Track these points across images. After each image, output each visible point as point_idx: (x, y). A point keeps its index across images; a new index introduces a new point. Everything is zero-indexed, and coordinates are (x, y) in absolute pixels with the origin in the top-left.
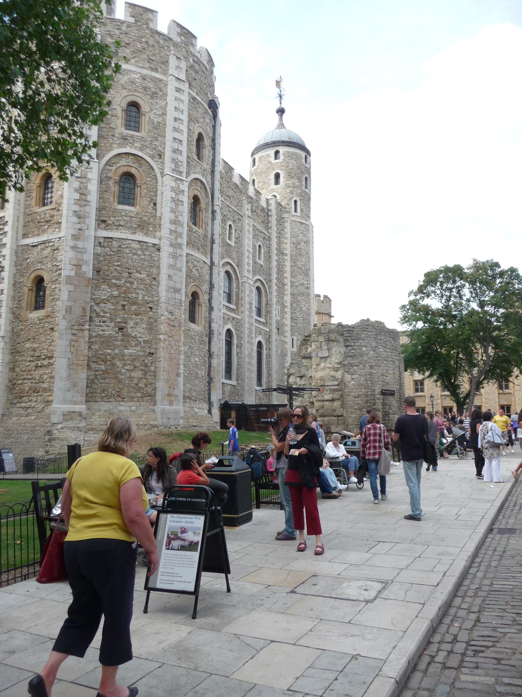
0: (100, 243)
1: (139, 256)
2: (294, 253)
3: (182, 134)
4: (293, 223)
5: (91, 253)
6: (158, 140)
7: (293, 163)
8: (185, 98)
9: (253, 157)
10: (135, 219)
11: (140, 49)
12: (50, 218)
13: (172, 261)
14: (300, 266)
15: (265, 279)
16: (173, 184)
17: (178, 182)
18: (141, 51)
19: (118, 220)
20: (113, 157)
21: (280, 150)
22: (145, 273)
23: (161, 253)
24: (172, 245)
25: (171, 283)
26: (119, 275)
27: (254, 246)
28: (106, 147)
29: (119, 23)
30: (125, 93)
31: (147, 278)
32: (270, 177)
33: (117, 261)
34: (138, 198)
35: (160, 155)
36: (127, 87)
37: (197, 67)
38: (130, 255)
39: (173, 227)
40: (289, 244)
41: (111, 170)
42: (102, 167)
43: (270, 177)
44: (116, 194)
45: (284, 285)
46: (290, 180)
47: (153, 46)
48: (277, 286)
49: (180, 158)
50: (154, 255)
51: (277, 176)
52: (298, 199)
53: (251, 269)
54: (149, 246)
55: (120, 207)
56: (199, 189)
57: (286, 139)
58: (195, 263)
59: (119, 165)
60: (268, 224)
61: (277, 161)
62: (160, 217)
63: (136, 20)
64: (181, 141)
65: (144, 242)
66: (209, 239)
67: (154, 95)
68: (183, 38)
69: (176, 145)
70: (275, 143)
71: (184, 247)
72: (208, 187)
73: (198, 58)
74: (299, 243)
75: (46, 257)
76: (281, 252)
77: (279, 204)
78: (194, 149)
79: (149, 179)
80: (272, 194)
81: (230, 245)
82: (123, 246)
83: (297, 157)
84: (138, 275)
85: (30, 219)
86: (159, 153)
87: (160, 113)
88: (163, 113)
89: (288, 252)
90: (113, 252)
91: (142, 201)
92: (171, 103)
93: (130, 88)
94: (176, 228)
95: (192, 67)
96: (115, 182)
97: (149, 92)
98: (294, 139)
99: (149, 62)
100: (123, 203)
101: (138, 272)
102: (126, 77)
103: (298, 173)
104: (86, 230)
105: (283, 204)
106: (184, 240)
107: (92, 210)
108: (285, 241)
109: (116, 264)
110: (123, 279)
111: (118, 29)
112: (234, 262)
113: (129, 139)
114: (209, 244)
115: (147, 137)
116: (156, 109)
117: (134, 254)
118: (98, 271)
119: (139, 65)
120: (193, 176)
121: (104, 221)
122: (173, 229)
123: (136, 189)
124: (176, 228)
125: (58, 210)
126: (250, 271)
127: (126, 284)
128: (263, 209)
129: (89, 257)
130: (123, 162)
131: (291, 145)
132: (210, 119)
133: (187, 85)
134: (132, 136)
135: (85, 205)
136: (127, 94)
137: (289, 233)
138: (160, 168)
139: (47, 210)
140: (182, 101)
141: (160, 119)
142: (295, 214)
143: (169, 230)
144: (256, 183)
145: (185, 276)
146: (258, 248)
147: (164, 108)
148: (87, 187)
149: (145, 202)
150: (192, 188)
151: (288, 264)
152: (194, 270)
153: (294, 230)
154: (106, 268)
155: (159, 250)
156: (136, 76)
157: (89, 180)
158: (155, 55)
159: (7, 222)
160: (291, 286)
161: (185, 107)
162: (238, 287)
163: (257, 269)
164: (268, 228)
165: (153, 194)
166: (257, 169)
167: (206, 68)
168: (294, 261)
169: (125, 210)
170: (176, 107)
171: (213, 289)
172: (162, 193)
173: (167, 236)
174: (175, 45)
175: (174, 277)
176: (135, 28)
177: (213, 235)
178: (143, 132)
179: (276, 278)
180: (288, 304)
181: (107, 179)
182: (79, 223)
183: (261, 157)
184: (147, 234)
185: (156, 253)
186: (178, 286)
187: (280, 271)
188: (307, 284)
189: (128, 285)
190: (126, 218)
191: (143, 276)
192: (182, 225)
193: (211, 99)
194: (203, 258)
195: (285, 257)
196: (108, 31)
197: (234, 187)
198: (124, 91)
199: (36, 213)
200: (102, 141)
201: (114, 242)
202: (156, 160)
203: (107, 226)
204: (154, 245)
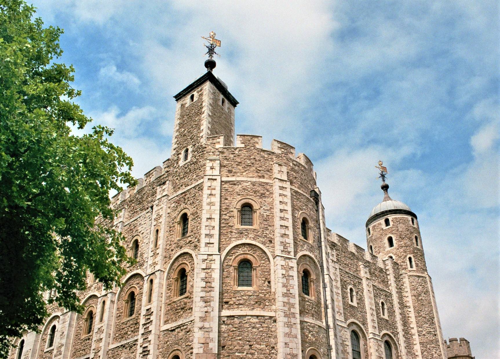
0: (224, 321)
1: (258, 329)
2: (416, 304)
3: (288, 221)
4: (411, 278)
5: (216, 332)
6: (268, 229)
7: (401, 227)
8: (288, 193)
9: (368, 227)
10: (252, 297)
11: (250, 164)
12: (184, 305)
13: (287, 330)
14: (424, 315)
15: (392, 333)
16: (283, 263)
17: (287, 261)
18: (251, 166)
19: (238, 300)
20: (232, 248)
21: (389, 218)
22: (264, 344)
23: (277, 324)
24: (286, 316)
25: (288, 351)
26: (241, 348)
27: (377, 304)
29: (233, 150)
30: (239, 198)
31: (267, 348)
32: (385, 242)
33: (239, 336)
34: (255, 279)
35: (271, 241)
36: (241, 193)
37: (297, 168)
38: (250, 329)
39: (286, 300)
40: (410, 297)
41: (231, 259)
43: (385, 242)
44: (235, 278)
45: (412, 335)
46: (401, 241)
47: (260, 160)
48: (406, 338)
49: (288, 240)
50: (271, 327)
51: (390, 240)
52: (411, 256)
53: (376, 325)
54: (266, 319)
55: (240, 288)
56: (308, 263)
57: (393, 208)
58: (311, 329)
59: (237, 254)
60: (388, 282)
61: (388, 227)
62: (274, 293)
63: (245, 146)
64: (287, 227)
65: (262, 316)
66: (323, 305)
67: (262, 196)
68: (283, 150)
69: (283, 231)
70: (384, 213)
71: (298, 316)
72: (316, 261)
73: (297, 162)
74: (419, 295)
75: (181, 339)
76: (403, 305)
77: (396, 264)
78: (300, 231)
79: (263, 262)
80: (388, 256)
81: (352, 307)
82: (243, 322)
83: (405, 221)
84: (258, 346)
85: (170, 308)
86: (269, 239)
87: (268, 208)
88: (271, 208)
89: (410, 304)
90: (235, 328)
91: (257, 281)
92: (277, 199)
93: (243, 193)
94: (289, 300)
95: (292, 169)
96: (235, 269)
97: (258, 194)
98: (399, 207)
99: (257, 172)
100: (243, 285)
101: (258, 343)
102: (240, 186)
103: (408, 234)
104: (212, 313)
105: (399, 262)
106: (297, 311)
107: (216, 294)
108: (406, 295)
109: (238, 338)
110: (245, 352)
111: (232, 154)
112: (360, 321)
113: (244, 232)
114: (323, 310)
115: (259, 228)
116: (265, 205)
117: (253, 328)
118: (223, 347)
119: (249, 175)
120: (300, 254)
121: (227, 303)
122: (287, 301)
123: (253, 272)
124: (289, 300)
125: (190, 298)
126: (375, 327)
127: (248, 355)
128: (381, 270)
129: (214, 335)
130: (240, 251)
131: (398, 212)
132: (313, 206)
133: (289, 183)
134: (246, 230)
135: (210, 291)
136: (241, 198)
137: (408, 287)
138: (271, 252)
139: (182, 299)
140: (285, 196)
141: (268, 213)
142: (411, 269)
143: (282, 303)
144: (373, 249)
145: (300, 342)
146: (380, 305)
147: (271, 204)
148: (211, 275)
149: (260, 282)
150: (301, 264)
151: (412, 315)
152: (310, 335)
153: (413, 284)
154: (230, 343)
155: (275, 321)
156: (248, 184)
158: (261, 167)
159: (152, 312)
160: (419, 335)
161: (288, 200)
162: (366, 344)
163: (382, 323)
164: (387, 285)
165: (267, 273)
166: (372, 237)
167: (305, 168)
168: (418, 312)
169: (244, 291)
170: (280, 202)
171: (331, 351)
172: (275, 272)
173: (281, 308)
174: (278, 156)
175: (290, 344)
176: (245, 150)
177: (326, 301)
178: (255, 225)
179: (403, 330)
180: (419, 353)
181: (228, 267)
182: (206, 307)
183: (374, 227)
184: (263, 308)
185: (273, 324)
186: (295, 352)
187: (405, 323)
188: (434, 331)
189: (250, 356)
190: (245, 297)
191: (262, 346)
192: (294, 297)
193: (312, 190)
194: (318, 323)
195: (409, 310)
196: (225, 157)
197: (351, 256)
198: (239, 196)
199: (174, 302)
201: (235, 319)
202: (267, 245)
203: (230, 306)
204: (271, 317)
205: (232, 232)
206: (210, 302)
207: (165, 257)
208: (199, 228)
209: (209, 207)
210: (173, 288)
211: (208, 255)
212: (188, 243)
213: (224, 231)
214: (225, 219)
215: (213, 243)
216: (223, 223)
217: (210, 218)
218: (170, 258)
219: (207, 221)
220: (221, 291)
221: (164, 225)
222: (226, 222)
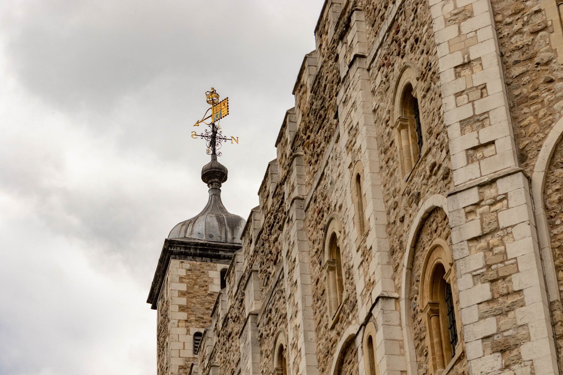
28: (538, 120)
42: (538, 177)
135: (511, 308)
148: (505, 253)
157: (508, 230)
200: (526, 110)
205: (551, 81)
206: (516, 345)
207: (393, 252)
208: (438, 113)
209: (456, 27)
210: (427, 342)
211: (481, 186)
212: (430, 176)
213: (525, 90)
214: (518, 48)
215: (493, 143)
216: (516, 62)
217: (466, 64)
218: (402, 248)
219: (458, 76)
220: (555, 296)
221: (367, 154)
222: (525, 56)
